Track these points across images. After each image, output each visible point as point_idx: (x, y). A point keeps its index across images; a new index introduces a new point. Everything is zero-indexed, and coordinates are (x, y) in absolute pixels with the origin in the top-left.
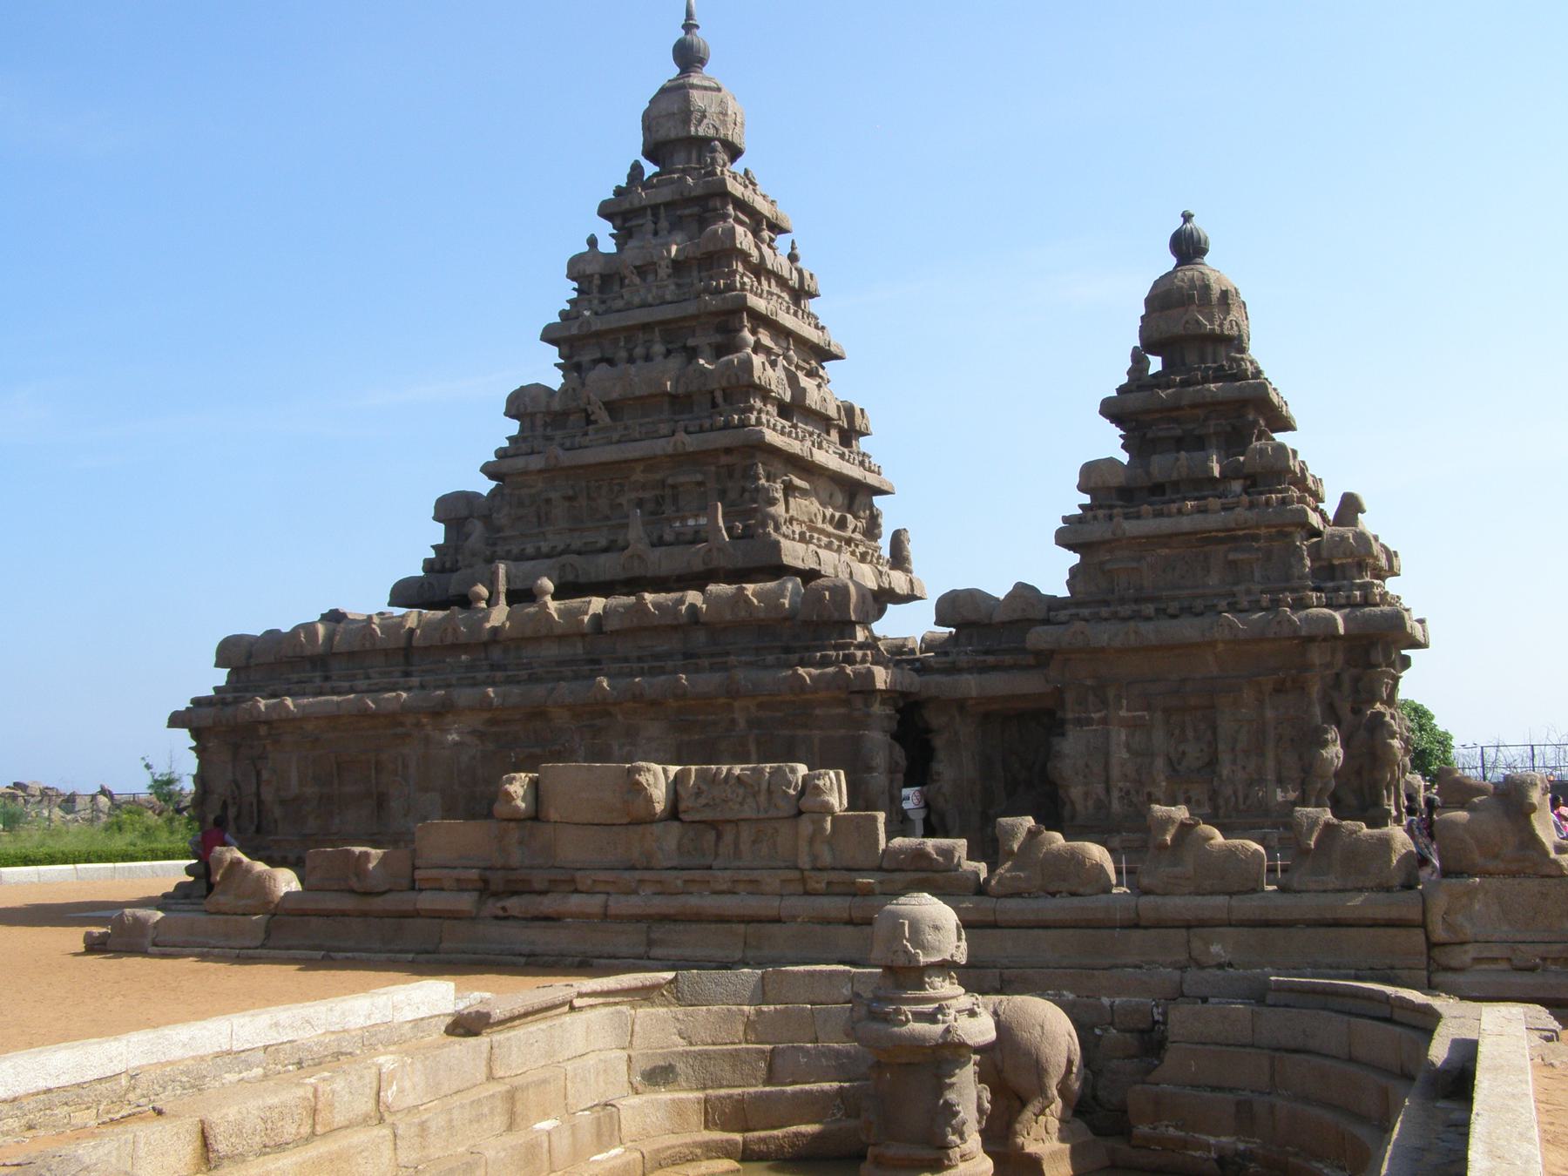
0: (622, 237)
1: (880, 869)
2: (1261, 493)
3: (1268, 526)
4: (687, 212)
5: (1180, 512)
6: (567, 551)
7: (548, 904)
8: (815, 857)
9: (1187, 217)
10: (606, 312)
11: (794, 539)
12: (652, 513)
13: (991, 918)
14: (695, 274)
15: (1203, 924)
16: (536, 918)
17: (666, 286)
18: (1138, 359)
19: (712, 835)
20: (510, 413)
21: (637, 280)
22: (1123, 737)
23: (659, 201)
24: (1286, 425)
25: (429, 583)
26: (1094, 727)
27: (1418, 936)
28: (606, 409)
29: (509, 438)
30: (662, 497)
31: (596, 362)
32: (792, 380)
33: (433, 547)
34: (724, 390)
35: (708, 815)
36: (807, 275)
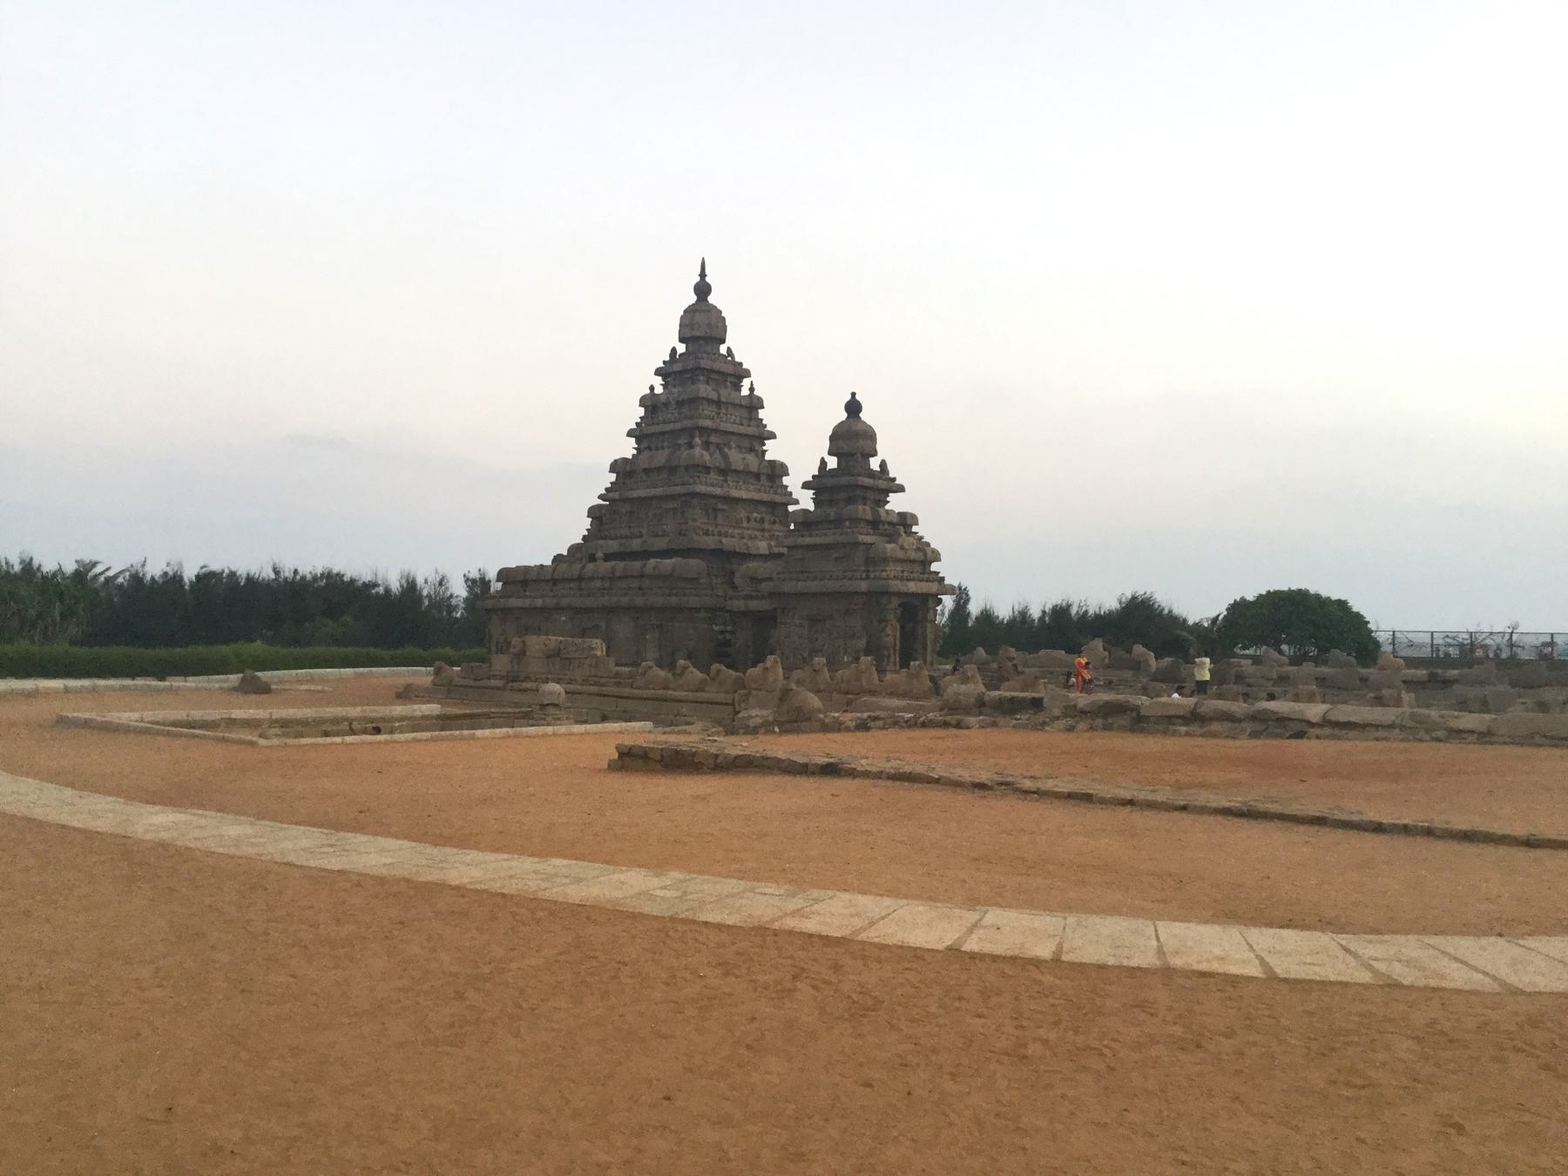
0: (665, 386)
1: (607, 677)
2: (848, 528)
4: (686, 376)
5: (817, 535)
6: (626, 537)
7: (524, 685)
9: (853, 394)
11: (713, 535)
12: (659, 521)
13: (631, 696)
16: (520, 690)
18: (823, 463)
19: (567, 662)
20: (611, 471)
21: (664, 410)
24: (901, 489)
27: (730, 709)
29: (611, 483)
31: (646, 448)
32: (726, 457)
33: (588, 530)
35: (569, 656)
36: (755, 400)
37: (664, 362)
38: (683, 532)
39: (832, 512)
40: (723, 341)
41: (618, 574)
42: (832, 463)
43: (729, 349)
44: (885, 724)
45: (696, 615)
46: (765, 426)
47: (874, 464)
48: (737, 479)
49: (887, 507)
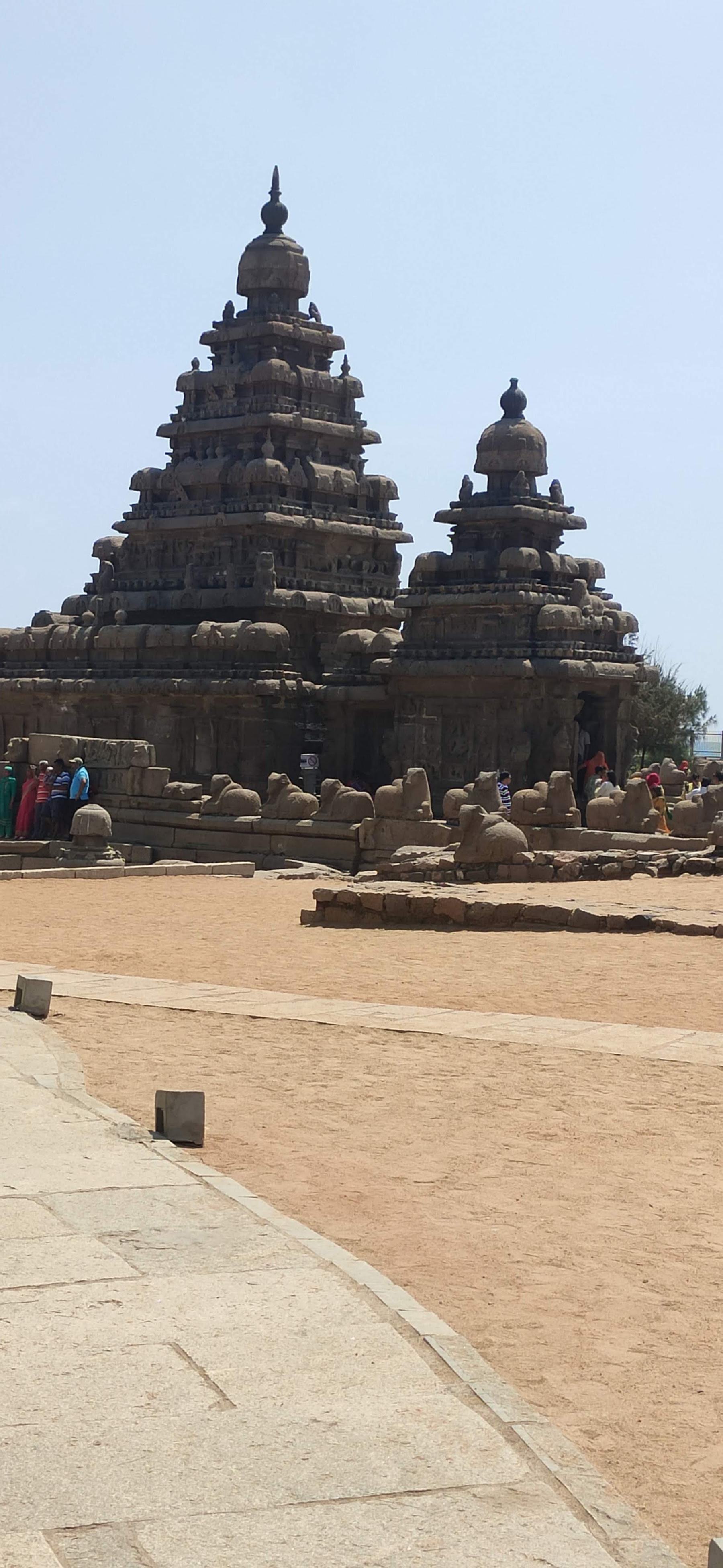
0: (216, 361)
1: (161, 797)
3: (505, 604)
4: (251, 347)
5: (459, 591)
6: (156, 588)
8: (133, 790)
10: (198, 418)
14: (252, 393)
15: (277, 834)
17: (232, 403)
18: (467, 485)
21: (216, 397)
22: (424, 732)
23: (236, 338)
24: (580, 525)
25: (83, 602)
26: (410, 724)
27: (353, 845)
28: (185, 490)
29: (132, 506)
30: (214, 553)
31: (186, 455)
32: (310, 471)
33: (91, 575)
34: (251, 483)
37: (215, 324)
38: (247, 582)
39: (480, 558)
40: (304, 294)
41: (151, 643)
42: (480, 483)
43: (312, 307)
44: (623, 868)
45: (275, 706)
46: (365, 424)
47: (542, 485)
48: (325, 505)
49: (560, 550)
